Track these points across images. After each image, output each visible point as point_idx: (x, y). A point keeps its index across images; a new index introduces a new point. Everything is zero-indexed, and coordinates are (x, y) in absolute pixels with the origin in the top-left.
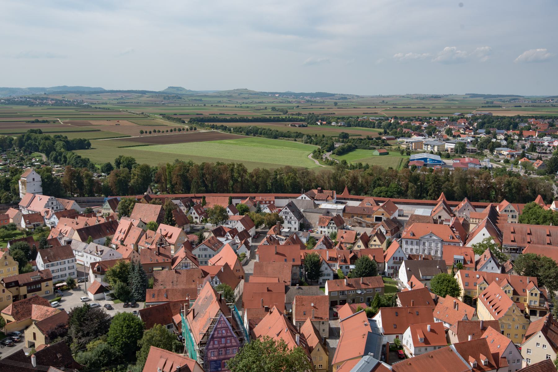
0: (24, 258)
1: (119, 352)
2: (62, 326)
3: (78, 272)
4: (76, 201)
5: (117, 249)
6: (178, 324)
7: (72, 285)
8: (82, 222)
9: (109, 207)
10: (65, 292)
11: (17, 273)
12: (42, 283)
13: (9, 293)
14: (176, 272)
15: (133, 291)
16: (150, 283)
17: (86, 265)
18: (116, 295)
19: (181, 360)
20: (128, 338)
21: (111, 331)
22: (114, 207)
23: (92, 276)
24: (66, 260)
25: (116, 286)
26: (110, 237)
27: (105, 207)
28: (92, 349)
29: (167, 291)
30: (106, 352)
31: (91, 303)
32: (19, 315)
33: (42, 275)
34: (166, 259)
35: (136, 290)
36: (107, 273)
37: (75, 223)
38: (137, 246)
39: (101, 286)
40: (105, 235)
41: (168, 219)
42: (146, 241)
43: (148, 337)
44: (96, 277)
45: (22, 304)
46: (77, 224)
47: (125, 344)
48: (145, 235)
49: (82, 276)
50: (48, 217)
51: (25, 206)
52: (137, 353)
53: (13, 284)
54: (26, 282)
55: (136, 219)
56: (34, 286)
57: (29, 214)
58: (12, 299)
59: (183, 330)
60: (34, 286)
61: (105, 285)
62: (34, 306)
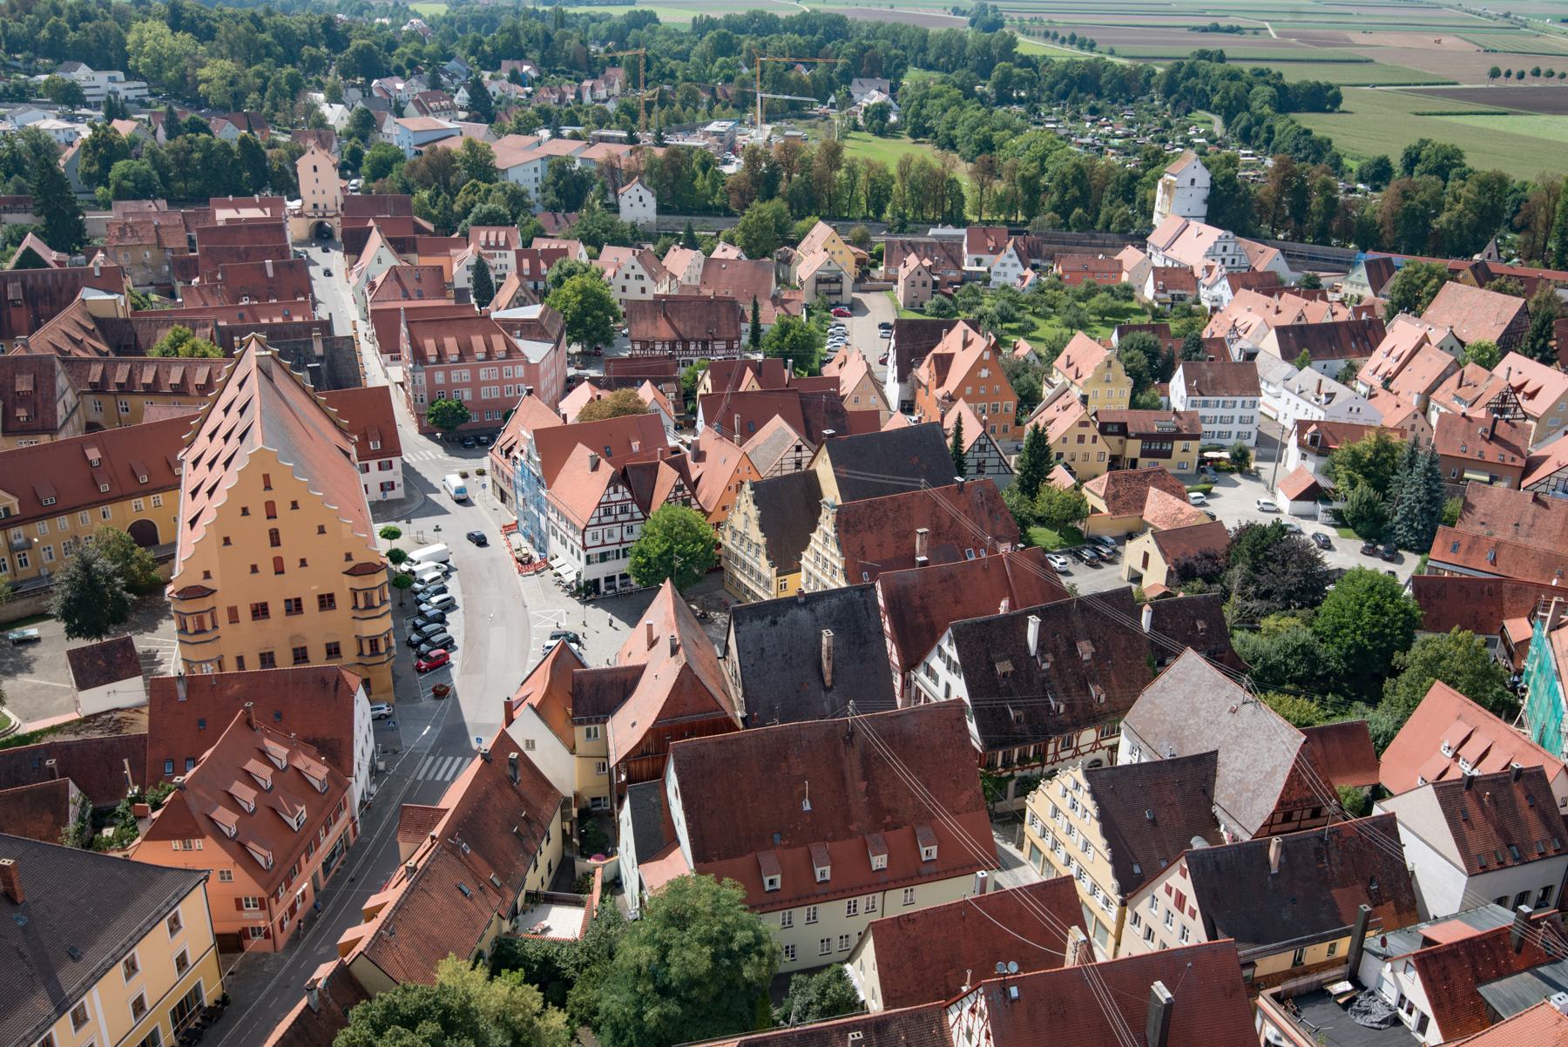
0: (1148, 372)
1: (1338, 662)
2: (1210, 557)
3: (1260, 434)
4: (1283, 251)
5: (1371, 397)
6: (1517, 644)
7: (1240, 463)
8: (1292, 308)
9: (1365, 279)
10: (1221, 476)
11: (1125, 405)
12: (1177, 443)
13: (1104, 447)
14: (1536, 499)
15: (1397, 518)
16: (1448, 510)
17: (1281, 420)
18: (1348, 517)
19: (1517, 744)
20: (1372, 637)
21: (1325, 606)
22: (1377, 283)
23: (1293, 451)
24: (1239, 400)
25: (1353, 496)
26: (1357, 361)
27: (1353, 277)
28: (1273, 633)
29: (1498, 545)
30: (1305, 651)
31: (1286, 519)
32: (1119, 503)
33: (1179, 423)
34: (1510, 455)
35: (1404, 519)
36: (1337, 456)
37: (1273, 309)
38: (1428, 401)
39: (1315, 484)
40: (1343, 352)
41: (1534, 341)
42: (1459, 392)
43: (1430, 654)
44: (1304, 457)
45: (1128, 478)
46: (1278, 312)
47: (1361, 649)
48: (1458, 375)
49: (1270, 447)
50: (1208, 282)
51: (1161, 245)
52: (1388, 683)
53: (1116, 429)
54: (1144, 431)
55: (1435, 325)
56: (1158, 445)
57: (1166, 268)
58: (1107, 461)
59: (1529, 665)
60: (1158, 445)
61: (1324, 483)
62: (1153, 491)
